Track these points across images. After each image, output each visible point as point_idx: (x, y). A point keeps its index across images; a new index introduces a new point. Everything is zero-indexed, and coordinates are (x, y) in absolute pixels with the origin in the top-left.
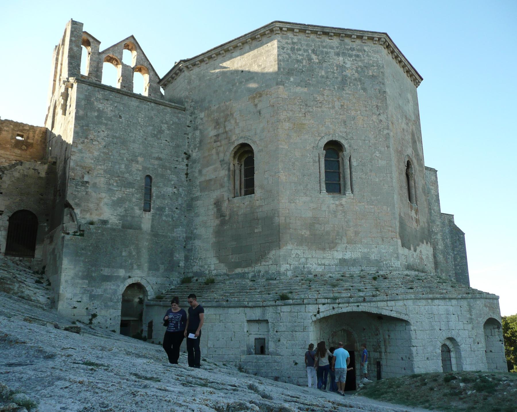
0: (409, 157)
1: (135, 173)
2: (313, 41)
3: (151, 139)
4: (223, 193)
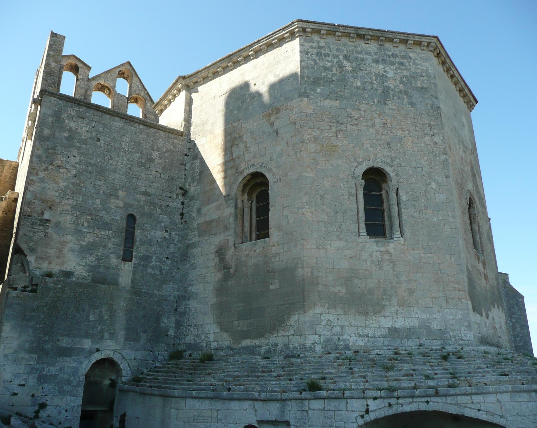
0: (470, 193)
1: (113, 210)
2: (345, 45)
3: (138, 169)
4: (228, 238)
